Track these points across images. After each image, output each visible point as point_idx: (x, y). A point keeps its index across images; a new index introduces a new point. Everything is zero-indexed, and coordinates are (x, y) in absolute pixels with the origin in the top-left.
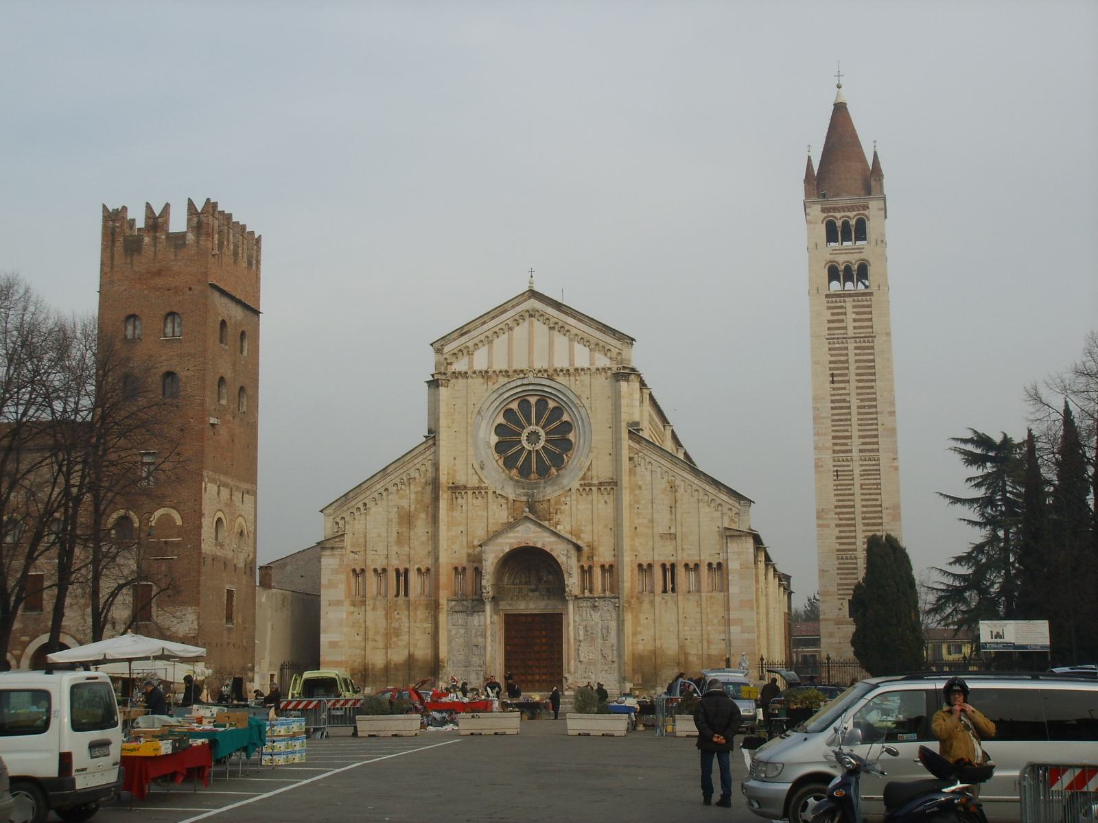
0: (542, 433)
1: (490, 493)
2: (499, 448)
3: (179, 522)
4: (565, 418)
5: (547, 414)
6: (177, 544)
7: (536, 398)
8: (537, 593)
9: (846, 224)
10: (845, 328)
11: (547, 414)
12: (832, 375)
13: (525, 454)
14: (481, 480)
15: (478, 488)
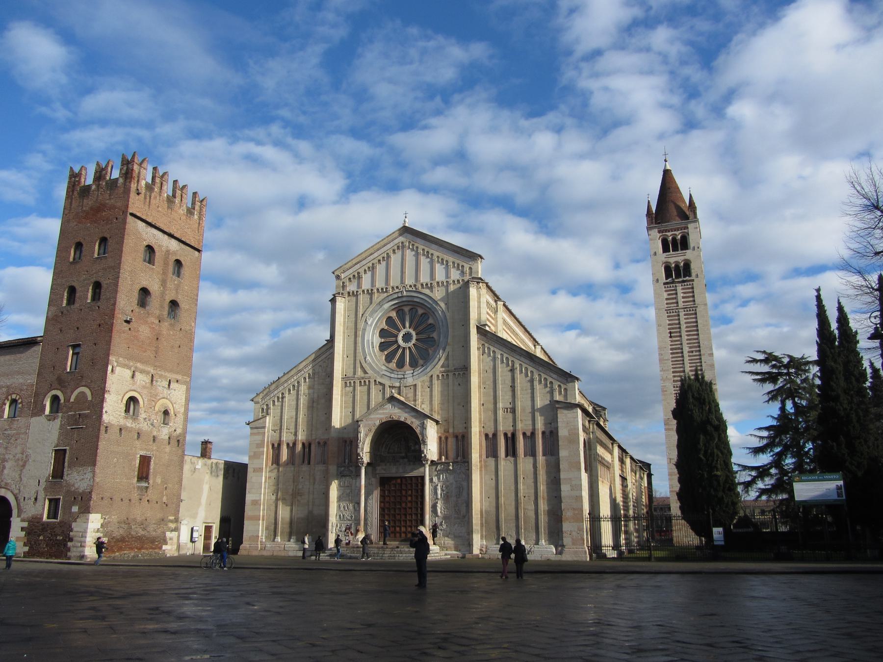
0: (414, 333)
1: (372, 381)
2: (383, 347)
3: (90, 398)
4: (431, 321)
5: (417, 319)
6: (86, 416)
7: (409, 307)
8: (406, 460)
9: (674, 239)
10: (677, 303)
11: (417, 319)
12: (670, 333)
13: (400, 351)
14: (365, 372)
15: (363, 378)
